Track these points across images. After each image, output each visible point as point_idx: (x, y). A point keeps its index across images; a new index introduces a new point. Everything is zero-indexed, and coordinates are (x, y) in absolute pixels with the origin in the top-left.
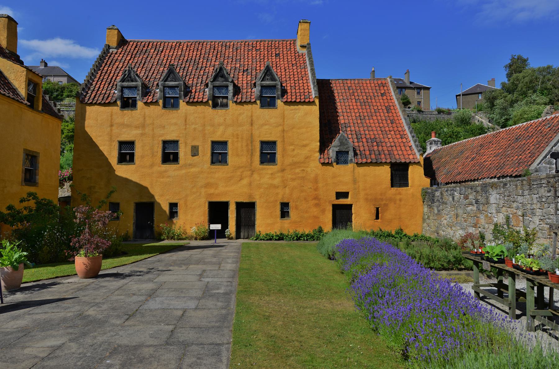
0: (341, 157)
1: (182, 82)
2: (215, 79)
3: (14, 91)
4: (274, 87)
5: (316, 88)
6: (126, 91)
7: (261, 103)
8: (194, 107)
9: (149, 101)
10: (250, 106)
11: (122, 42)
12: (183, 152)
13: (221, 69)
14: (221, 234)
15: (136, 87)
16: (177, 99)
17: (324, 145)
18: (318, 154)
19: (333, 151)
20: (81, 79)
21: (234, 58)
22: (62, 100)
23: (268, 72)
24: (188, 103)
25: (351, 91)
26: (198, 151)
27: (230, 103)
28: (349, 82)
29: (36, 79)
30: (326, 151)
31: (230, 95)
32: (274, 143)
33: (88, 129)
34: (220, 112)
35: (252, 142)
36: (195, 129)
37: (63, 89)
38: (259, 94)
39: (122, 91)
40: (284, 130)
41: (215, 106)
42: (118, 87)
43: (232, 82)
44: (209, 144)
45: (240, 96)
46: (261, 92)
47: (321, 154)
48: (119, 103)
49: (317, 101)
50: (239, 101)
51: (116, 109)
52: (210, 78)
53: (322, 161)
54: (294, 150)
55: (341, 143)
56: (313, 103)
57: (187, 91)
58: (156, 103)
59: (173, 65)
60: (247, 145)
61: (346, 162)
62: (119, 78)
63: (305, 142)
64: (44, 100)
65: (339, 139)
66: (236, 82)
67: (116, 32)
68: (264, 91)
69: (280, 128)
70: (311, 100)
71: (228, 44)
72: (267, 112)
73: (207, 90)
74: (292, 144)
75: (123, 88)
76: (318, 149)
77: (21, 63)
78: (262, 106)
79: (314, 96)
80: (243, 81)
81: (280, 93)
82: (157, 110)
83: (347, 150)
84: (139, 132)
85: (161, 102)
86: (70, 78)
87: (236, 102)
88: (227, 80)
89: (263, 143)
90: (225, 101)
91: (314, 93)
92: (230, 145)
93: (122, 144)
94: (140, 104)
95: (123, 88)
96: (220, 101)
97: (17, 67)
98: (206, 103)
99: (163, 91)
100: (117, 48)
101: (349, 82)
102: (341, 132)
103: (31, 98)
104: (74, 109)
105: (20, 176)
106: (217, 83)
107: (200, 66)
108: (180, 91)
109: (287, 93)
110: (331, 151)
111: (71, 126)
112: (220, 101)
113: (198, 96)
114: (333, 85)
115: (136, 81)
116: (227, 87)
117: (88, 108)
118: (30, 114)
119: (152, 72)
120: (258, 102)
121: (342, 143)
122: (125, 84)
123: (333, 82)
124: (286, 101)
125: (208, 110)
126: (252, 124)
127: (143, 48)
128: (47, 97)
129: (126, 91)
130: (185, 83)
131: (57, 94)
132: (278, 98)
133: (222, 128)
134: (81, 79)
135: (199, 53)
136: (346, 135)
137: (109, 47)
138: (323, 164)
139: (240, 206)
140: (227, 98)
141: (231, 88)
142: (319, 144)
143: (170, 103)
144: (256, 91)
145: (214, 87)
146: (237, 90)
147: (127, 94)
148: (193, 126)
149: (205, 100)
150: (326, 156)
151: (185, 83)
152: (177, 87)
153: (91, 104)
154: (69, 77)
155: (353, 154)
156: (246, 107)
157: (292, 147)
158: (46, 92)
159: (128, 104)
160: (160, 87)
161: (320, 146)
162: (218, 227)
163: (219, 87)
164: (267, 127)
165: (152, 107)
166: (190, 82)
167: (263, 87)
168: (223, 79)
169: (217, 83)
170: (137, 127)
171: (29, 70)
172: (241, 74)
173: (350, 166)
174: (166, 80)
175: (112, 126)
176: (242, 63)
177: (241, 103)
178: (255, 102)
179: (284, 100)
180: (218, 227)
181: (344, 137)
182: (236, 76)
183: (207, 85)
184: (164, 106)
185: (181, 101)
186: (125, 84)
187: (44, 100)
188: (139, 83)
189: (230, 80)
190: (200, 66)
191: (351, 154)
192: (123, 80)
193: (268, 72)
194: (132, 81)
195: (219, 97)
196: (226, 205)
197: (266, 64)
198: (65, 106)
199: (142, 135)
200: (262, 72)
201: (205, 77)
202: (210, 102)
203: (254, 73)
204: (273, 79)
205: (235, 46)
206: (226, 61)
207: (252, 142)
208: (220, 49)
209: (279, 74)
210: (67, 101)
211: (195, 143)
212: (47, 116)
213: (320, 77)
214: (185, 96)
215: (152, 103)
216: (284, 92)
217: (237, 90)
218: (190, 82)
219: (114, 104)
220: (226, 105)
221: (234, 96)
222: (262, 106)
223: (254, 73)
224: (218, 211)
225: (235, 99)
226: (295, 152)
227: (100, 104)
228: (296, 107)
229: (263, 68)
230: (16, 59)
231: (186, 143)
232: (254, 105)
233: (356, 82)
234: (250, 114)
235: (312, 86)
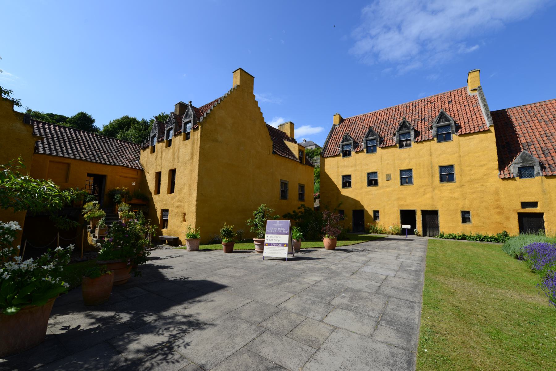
0: (525, 171)
1: (378, 136)
2: (400, 129)
3: (294, 156)
4: (449, 125)
5: (491, 119)
6: (345, 147)
7: (437, 139)
8: (386, 150)
10: (428, 143)
11: (342, 120)
12: (381, 178)
13: (404, 122)
14: (411, 232)
15: (350, 144)
16: (375, 147)
17: (503, 163)
18: (498, 171)
19: (514, 167)
20: (321, 144)
21: (414, 113)
22: (313, 157)
23: (442, 116)
24: (382, 148)
25: (532, 114)
26: (391, 177)
27: (413, 143)
28: (527, 107)
29: (302, 149)
30: (506, 168)
31: (412, 138)
32: (452, 166)
33: (326, 171)
34: (405, 150)
35: (432, 168)
36: (388, 163)
37: (314, 151)
38: (436, 133)
39: (343, 148)
40: (460, 156)
41: (401, 146)
42: (341, 146)
43: (413, 128)
44: (399, 172)
45: (420, 137)
46: (437, 131)
47: (500, 171)
48: (341, 154)
49: (492, 129)
50: (419, 141)
51: (340, 158)
52: (397, 129)
53: (503, 176)
54: (471, 170)
55: (523, 160)
56: (489, 131)
57: (381, 140)
58: (362, 151)
59: (371, 127)
60: (428, 170)
61: (531, 176)
62: (341, 141)
63: (482, 163)
64: (306, 158)
65: (521, 157)
66: (416, 128)
67: (338, 116)
68: (440, 130)
69: (457, 155)
70: (486, 129)
71: (408, 105)
72: (444, 145)
73: (395, 137)
74: (469, 166)
75: (343, 145)
76: (497, 167)
77: (296, 142)
78: (439, 141)
79: (488, 125)
80: (421, 127)
81: (454, 129)
82: (364, 155)
83: (531, 165)
84: (353, 169)
85: (365, 150)
86: (316, 146)
87: (417, 142)
88: (409, 128)
89: (441, 168)
90: (408, 142)
91: (488, 123)
92: (413, 171)
93: (344, 177)
94: (353, 153)
95: (343, 145)
96: (404, 143)
97: (295, 145)
98: (395, 146)
99: (366, 144)
100: (339, 125)
101: (527, 107)
102: (522, 150)
103: (300, 158)
104: (319, 161)
106: (402, 132)
107: (389, 123)
108: (377, 141)
109: (461, 128)
110: (511, 167)
111: (318, 170)
112: (404, 143)
113: (389, 143)
114: (510, 113)
116: (409, 133)
117: (326, 159)
118: (301, 167)
119: (359, 133)
120: (435, 139)
121: (524, 159)
122: (344, 143)
123: (509, 111)
124: (461, 134)
125: (397, 150)
126: (431, 155)
127: (353, 121)
128: (307, 157)
129: (345, 147)
130: (379, 136)
131: (311, 154)
132: (453, 133)
133: (407, 161)
134: (321, 144)
135: (388, 116)
136: (529, 152)
137: (335, 125)
138: (504, 179)
139: (424, 213)
140: (410, 140)
141: (412, 133)
142: (497, 163)
143: (371, 150)
144: (433, 132)
145: (400, 135)
146: (417, 134)
147: (346, 149)
148: (387, 162)
149: (393, 144)
150: (506, 172)
151: (379, 136)
152: (375, 139)
153: (327, 157)
154: (316, 145)
155: (539, 168)
156: (425, 143)
157: (470, 168)
158: (307, 154)
159: (346, 154)
160: (364, 141)
161: (499, 164)
162: (408, 227)
163: (403, 134)
164: (444, 155)
165: (360, 154)
166: (383, 135)
167: (438, 128)
169: (402, 132)
170: (352, 167)
171: (299, 145)
172: (419, 122)
173: (537, 179)
174: (367, 136)
175: (338, 167)
176: (420, 115)
177: (421, 142)
178: (433, 139)
179: (459, 134)
180: (408, 227)
181: (526, 154)
182: (416, 124)
183: (394, 135)
184: (367, 152)
185: (378, 148)
186: (344, 143)
187: (306, 158)
188: (352, 142)
189: (411, 128)
190: (389, 123)
191: (537, 168)
192: (343, 142)
193: (442, 116)
195: (404, 141)
196: (413, 212)
197: (440, 111)
198: (315, 160)
199: (355, 170)
200: (437, 117)
201: (393, 130)
202: (398, 145)
203: (430, 119)
204: (447, 120)
205: (414, 105)
206: (407, 116)
207: (432, 168)
208: (402, 109)
209: (452, 115)
210: (315, 158)
211: (388, 172)
212: (307, 166)
213: (493, 109)
214: (380, 144)
215: (360, 151)
216: (458, 127)
217: (417, 134)
218: (383, 135)
219: (339, 155)
220: (410, 145)
221: (415, 138)
222: (439, 141)
223: (430, 119)
224: (407, 216)
225: (416, 140)
226: (473, 172)
227: (332, 157)
228: (470, 137)
229: (437, 114)
230: (293, 141)
231: (382, 173)
232: (432, 142)
233: (538, 105)
234: (429, 148)
235: (486, 118)
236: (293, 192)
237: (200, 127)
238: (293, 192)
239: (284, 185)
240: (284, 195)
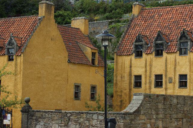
9: (148, 53)
16: (162, 51)
88: (187, 38)
92: (188, 77)
103: (93, 60)
105: (89, 97)
106: (182, 41)
115: (142, 42)
116: (187, 42)
145: (180, 43)
168: (185, 38)
169: (182, 41)
185: (164, 52)
186: (137, 43)
192: (136, 42)
194: (140, 42)
236: (85, 92)
237: (22, 55)
238: (85, 92)
239: (77, 87)
240: (77, 96)
